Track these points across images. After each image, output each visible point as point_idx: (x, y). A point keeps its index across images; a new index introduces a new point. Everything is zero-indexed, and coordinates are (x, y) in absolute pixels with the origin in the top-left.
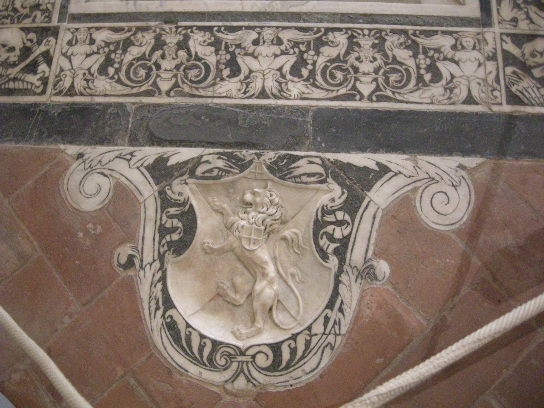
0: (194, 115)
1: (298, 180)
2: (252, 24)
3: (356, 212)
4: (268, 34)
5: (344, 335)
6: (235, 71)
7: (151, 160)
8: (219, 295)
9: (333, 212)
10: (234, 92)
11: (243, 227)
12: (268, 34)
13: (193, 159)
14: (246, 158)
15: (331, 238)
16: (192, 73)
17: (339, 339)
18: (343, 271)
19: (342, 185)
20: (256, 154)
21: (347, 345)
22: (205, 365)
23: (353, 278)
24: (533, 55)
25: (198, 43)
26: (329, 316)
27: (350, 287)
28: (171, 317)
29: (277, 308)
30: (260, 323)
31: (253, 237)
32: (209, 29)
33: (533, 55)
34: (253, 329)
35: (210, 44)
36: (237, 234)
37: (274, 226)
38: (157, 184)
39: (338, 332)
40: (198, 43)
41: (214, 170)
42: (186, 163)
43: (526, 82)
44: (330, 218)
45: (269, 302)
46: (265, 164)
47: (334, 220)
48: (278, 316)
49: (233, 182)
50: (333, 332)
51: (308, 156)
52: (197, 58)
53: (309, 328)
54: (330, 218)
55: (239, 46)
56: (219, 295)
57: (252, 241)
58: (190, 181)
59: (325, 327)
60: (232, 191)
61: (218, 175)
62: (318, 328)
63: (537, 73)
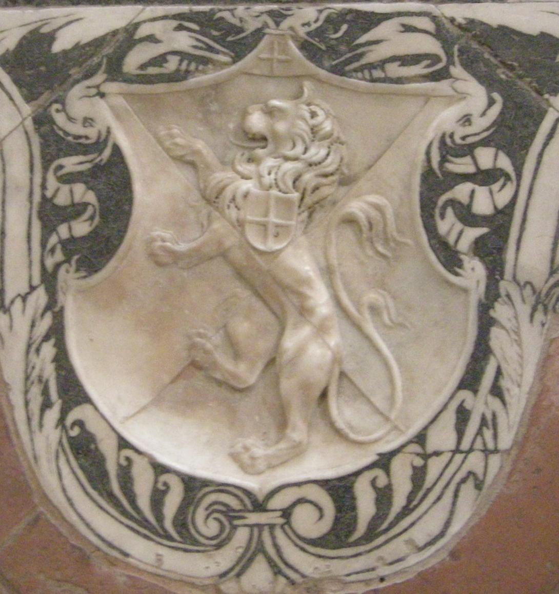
1: (377, 74)
3: (526, 147)
5: (508, 452)
7: (10, 42)
8: (196, 365)
9: (468, 150)
11: (246, 195)
13: (114, 33)
14: (246, 26)
15: (467, 216)
17: (495, 461)
18: (498, 296)
19: (488, 81)
20: (270, 13)
21: (515, 477)
22: (169, 538)
23: (524, 310)
26: (468, 405)
27: (517, 333)
28: (80, 423)
29: (339, 393)
30: (298, 432)
31: (273, 219)
34: (283, 445)
36: (233, 213)
37: (325, 191)
38: (29, 99)
39: (491, 446)
41: (169, 57)
42: (98, 43)
44: (462, 165)
45: (320, 378)
46: (295, 38)
47: (471, 169)
48: (343, 412)
49: (217, 86)
50: (479, 445)
51: (400, 14)
53: (420, 438)
54: (462, 165)
56: (195, 365)
57: (271, 230)
58: (111, 88)
59: (460, 432)
60: (214, 107)
61: (178, 70)
62: (443, 437)
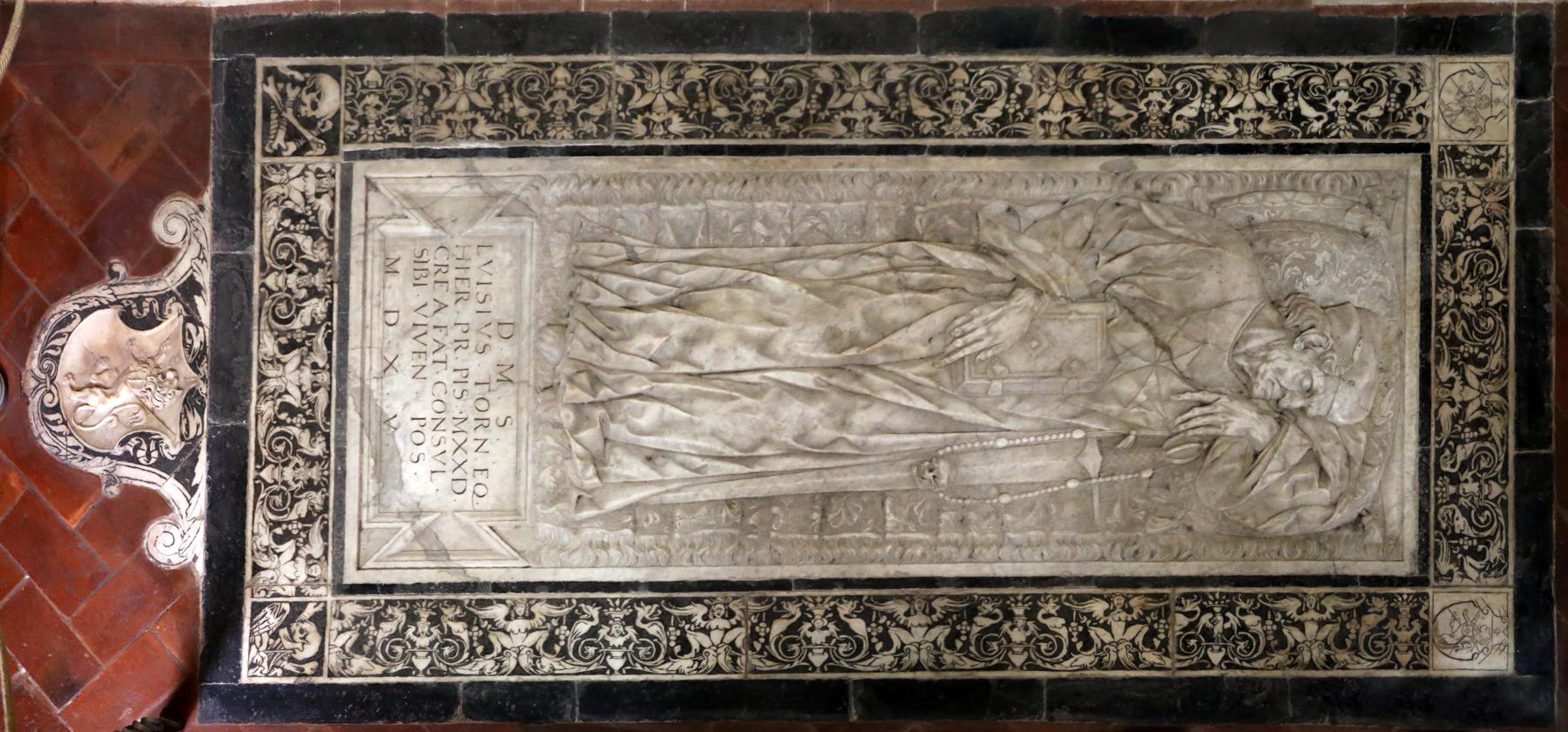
0: (242, 314)
2: (334, 360)
4: (323, 377)
6: (285, 349)
10: (263, 350)
12: (323, 377)
16: (283, 307)
24: (302, 631)
25: (317, 307)
32: (329, 318)
33: (302, 631)
35: (313, 320)
40: (317, 307)
43: (274, 621)
52: (298, 310)
55: (310, 349)
63: (284, 632)
